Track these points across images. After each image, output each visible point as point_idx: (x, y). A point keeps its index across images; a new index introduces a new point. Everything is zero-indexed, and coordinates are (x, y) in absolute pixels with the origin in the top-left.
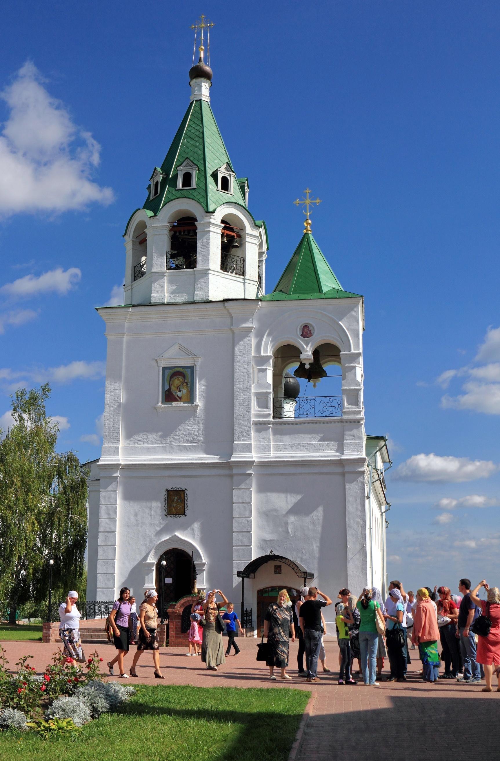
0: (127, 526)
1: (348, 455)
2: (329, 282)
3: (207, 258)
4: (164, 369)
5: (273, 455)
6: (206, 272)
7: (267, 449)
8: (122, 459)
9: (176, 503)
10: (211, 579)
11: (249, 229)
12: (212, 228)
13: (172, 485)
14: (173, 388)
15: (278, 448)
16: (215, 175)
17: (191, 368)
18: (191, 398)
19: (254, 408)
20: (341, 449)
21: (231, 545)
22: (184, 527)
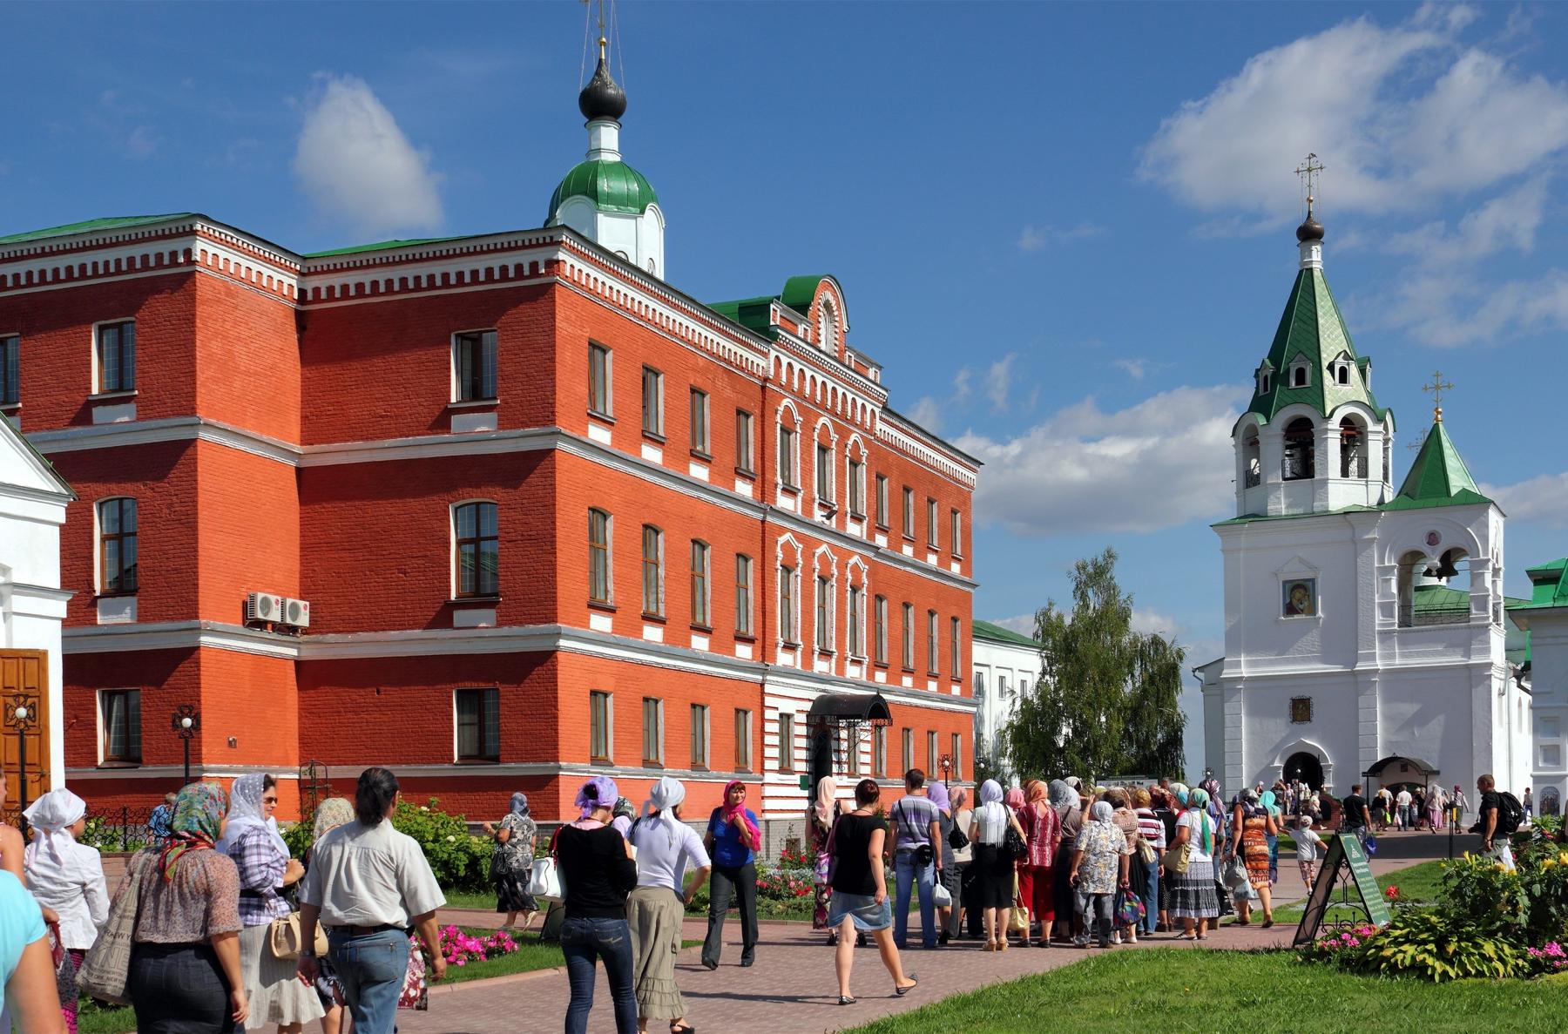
2: (1458, 480)
4: (1285, 583)
5: (1398, 662)
6: (1325, 482)
7: (1392, 656)
9: (1301, 710)
10: (1335, 780)
11: (1371, 426)
12: (1330, 435)
13: (1297, 694)
14: (1295, 602)
15: (1403, 656)
16: (1331, 367)
17: (1313, 581)
18: (1312, 610)
19: (1378, 618)
20: (1468, 654)
21: (1358, 748)
22: (1310, 735)
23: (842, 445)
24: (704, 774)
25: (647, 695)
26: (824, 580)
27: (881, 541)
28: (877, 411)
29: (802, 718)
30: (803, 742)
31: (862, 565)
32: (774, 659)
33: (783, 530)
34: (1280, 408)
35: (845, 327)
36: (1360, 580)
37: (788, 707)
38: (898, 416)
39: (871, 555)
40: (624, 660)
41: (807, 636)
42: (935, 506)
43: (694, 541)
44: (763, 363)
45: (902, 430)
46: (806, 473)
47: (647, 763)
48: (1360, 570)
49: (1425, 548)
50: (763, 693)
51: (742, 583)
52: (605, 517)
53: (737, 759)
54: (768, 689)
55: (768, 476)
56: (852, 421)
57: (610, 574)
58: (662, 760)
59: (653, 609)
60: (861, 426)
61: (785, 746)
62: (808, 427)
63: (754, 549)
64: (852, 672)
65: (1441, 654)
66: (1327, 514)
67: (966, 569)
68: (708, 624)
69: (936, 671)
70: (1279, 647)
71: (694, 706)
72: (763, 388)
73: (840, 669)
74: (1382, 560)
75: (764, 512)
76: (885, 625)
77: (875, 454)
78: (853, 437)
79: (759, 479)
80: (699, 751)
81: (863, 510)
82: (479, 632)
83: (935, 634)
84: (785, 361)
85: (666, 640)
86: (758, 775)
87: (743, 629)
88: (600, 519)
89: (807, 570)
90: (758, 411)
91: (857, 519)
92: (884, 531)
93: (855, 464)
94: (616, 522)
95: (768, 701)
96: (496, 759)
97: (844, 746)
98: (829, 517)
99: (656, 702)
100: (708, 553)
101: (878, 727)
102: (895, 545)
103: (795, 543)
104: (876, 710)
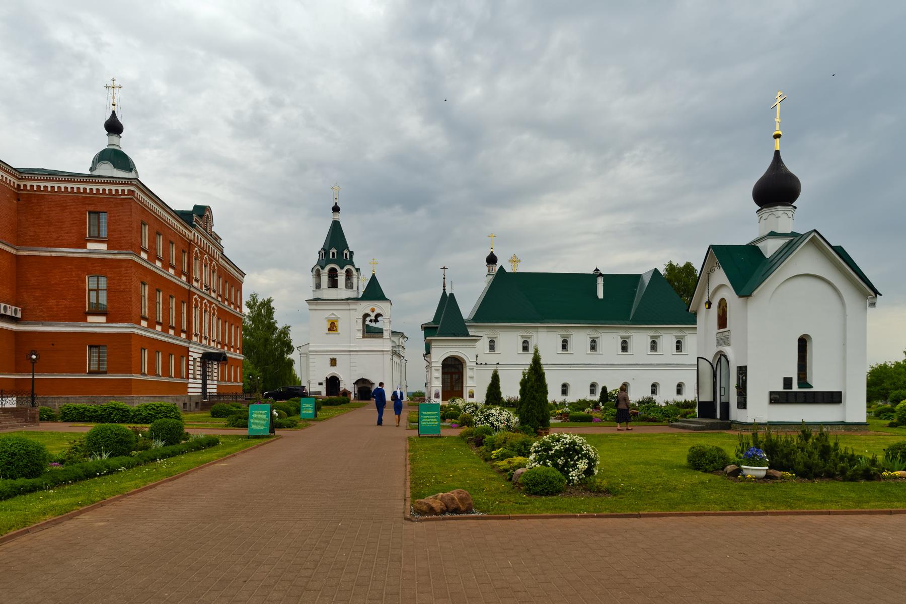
33: (195, 294)
49: (369, 312)
64: (212, 344)
89: (201, 308)
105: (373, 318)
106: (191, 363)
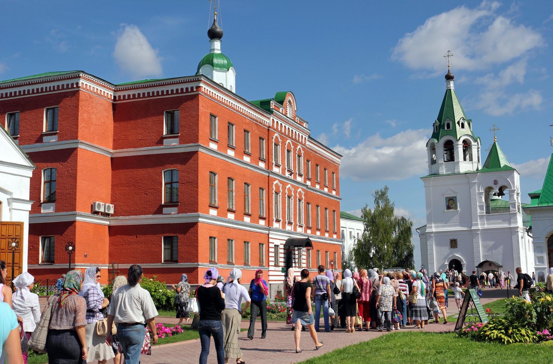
0: (437, 252)
1: (512, 226)
3: (458, 158)
4: (446, 198)
5: (486, 226)
6: (458, 162)
7: (484, 224)
8: (434, 230)
9: (454, 244)
14: (450, 205)
15: (488, 224)
17: (456, 197)
19: (479, 210)
20: (510, 224)
23: (295, 150)
24: (248, 267)
25: (229, 238)
26: (289, 197)
27: (308, 183)
28: (307, 138)
29: (282, 247)
30: (282, 255)
31: (302, 192)
32: (272, 225)
33: (275, 179)
34: (442, 137)
35: (296, 109)
36: (472, 197)
37: (277, 242)
38: (314, 140)
39: (305, 188)
40: (221, 226)
41: (284, 217)
42: (327, 171)
43: (245, 183)
44: (268, 121)
45: (315, 145)
46: (283, 159)
47: (229, 263)
48: (472, 193)
49: (494, 186)
50: (269, 237)
51: (261, 198)
52: (215, 175)
53: (260, 262)
54: (270, 236)
55: (270, 160)
56: (298, 141)
57: (217, 195)
58: (234, 262)
59: (231, 207)
60: (301, 143)
61: (276, 257)
62: (284, 143)
63: (265, 186)
64: (299, 230)
65: (499, 223)
66: (459, 174)
67: (338, 193)
68: (250, 213)
69: (328, 229)
70: (445, 221)
71: (245, 242)
72: (268, 130)
73: (295, 229)
74: (479, 190)
75: (269, 173)
76: (310, 213)
77: (306, 153)
78: (299, 147)
79: (267, 161)
80: (247, 259)
81: (302, 172)
82: (172, 216)
83: (327, 216)
84: (275, 120)
85: (235, 219)
86: (267, 267)
87: (262, 215)
88: (213, 176)
89: (284, 193)
90: (266, 138)
91: (300, 175)
92: (309, 180)
93: (299, 156)
94: (219, 176)
95: (271, 240)
96: (177, 262)
97: (297, 256)
98: (291, 175)
99: (232, 241)
100: (250, 187)
101: (308, 250)
102: (313, 185)
103: (279, 184)
104: (308, 243)
105: (497, 191)
106: (272, 250)
